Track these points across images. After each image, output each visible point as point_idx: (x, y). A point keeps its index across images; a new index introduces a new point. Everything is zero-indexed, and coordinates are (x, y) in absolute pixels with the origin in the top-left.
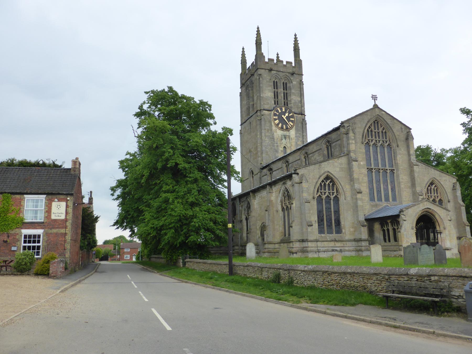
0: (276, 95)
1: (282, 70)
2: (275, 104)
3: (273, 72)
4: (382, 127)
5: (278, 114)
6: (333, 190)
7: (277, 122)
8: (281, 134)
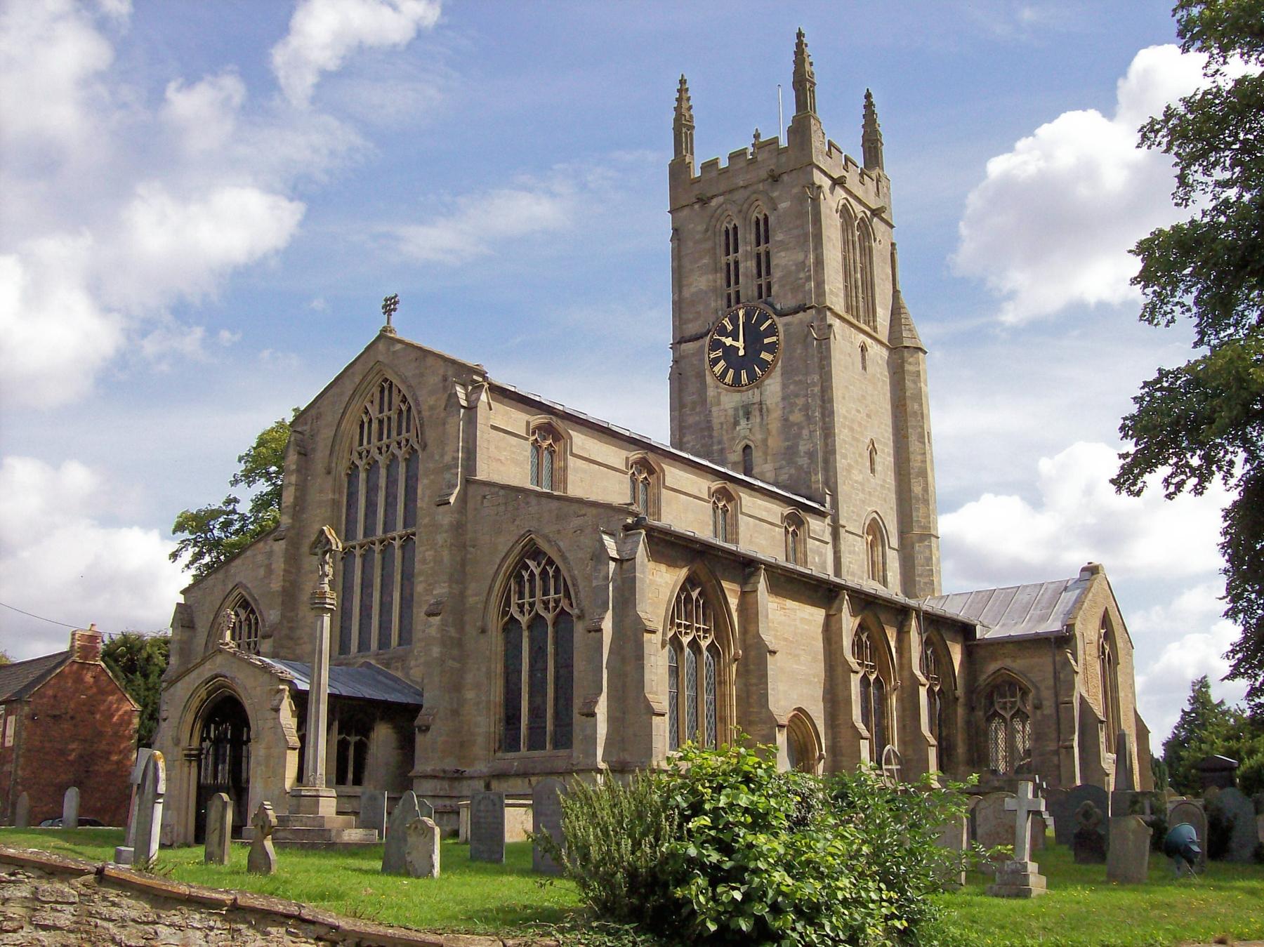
0: (732, 273)
1: (741, 184)
3: (714, 203)
8: (733, 405)
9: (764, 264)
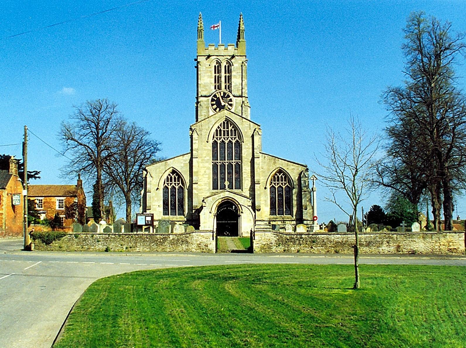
0: (218, 80)
2: (215, 88)
4: (232, 126)
5: (216, 99)
6: (179, 181)
7: (215, 106)
9: (229, 79)
